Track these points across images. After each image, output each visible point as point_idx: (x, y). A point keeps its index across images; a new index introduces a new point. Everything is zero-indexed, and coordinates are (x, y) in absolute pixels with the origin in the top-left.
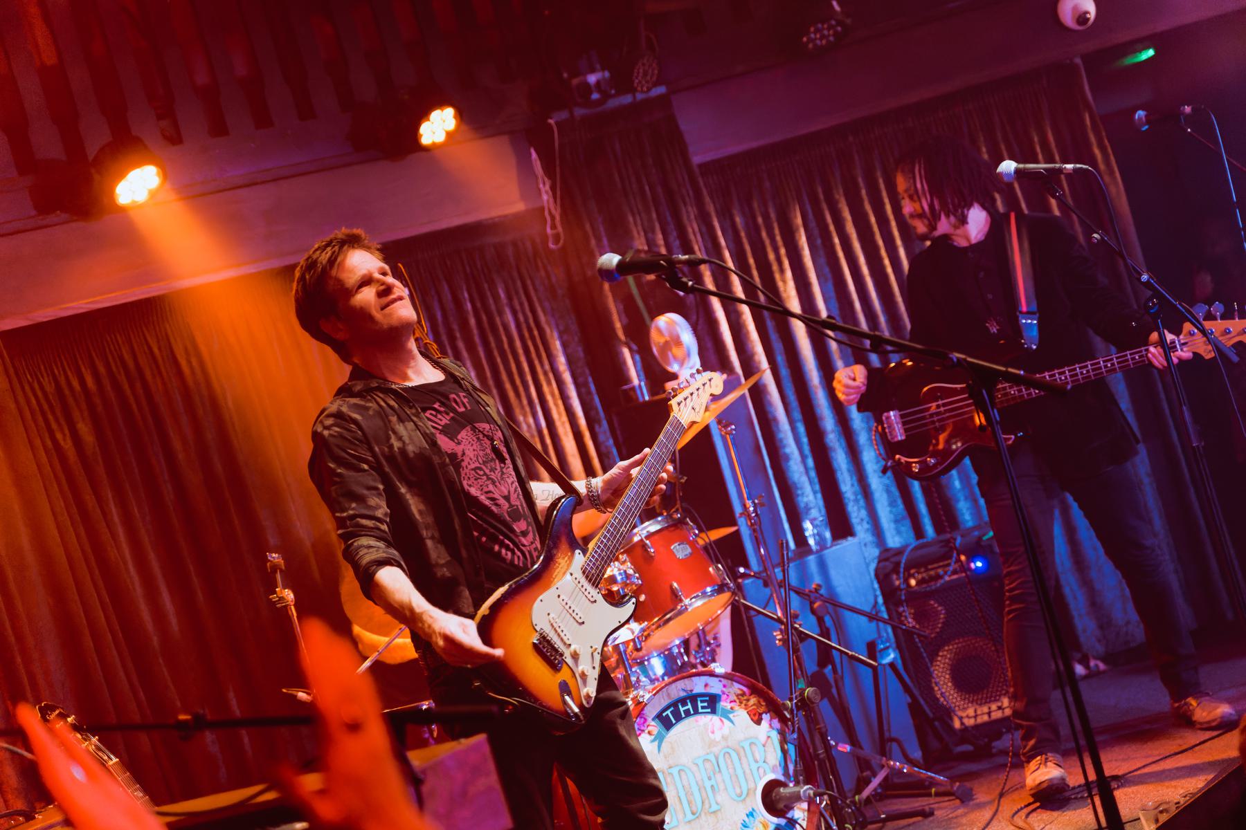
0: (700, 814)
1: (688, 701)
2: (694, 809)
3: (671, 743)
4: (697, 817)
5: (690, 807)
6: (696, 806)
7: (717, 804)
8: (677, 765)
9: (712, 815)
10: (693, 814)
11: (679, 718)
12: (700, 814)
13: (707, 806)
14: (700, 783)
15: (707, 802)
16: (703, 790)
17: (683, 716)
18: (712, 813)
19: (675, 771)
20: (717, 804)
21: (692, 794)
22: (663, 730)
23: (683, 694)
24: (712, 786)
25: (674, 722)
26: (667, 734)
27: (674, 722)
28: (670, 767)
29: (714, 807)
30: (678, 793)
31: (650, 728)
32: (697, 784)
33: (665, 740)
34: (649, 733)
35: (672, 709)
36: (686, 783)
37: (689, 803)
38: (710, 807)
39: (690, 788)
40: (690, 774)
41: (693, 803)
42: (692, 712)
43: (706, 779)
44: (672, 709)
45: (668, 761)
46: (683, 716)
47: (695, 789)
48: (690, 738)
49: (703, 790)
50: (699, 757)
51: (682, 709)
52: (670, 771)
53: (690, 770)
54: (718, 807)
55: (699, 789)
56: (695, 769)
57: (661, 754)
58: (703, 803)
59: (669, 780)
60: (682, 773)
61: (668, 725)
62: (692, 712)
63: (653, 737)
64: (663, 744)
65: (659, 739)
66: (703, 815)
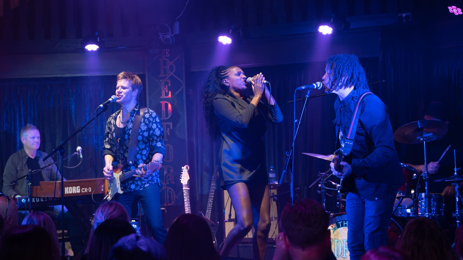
0: (339, 256)
1: (347, 222)
2: (338, 254)
3: (337, 232)
4: (338, 257)
5: (337, 253)
6: (339, 254)
7: (346, 255)
8: (337, 239)
9: (343, 258)
10: (337, 255)
11: (342, 226)
12: (339, 256)
13: (342, 255)
14: (343, 247)
15: (343, 254)
16: (343, 250)
17: (344, 225)
18: (343, 257)
19: (336, 241)
20: (346, 255)
21: (339, 250)
22: (336, 227)
23: (346, 219)
24: (346, 250)
25: (341, 226)
26: (337, 229)
27: (341, 226)
28: (335, 239)
29: (344, 256)
30: (335, 247)
31: (333, 225)
32: (342, 247)
33: (336, 230)
34: (332, 227)
35: (341, 222)
36: (338, 246)
37: (337, 251)
38: (343, 255)
39: (339, 247)
40: (340, 242)
41: (338, 253)
42: (347, 225)
43: (345, 246)
44: (341, 222)
45: (335, 237)
46: (344, 225)
47: (340, 248)
48: (344, 233)
49: (343, 250)
50: (345, 240)
51: (344, 223)
52: (335, 240)
53: (341, 242)
54: (345, 257)
55: (342, 249)
56: (342, 242)
57: (334, 234)
58: (341, 253)
59: (333, 242)
60: (338, 242)
61: (338, 227)
62: (347, 225)
63: (333, 228)
64: (335, 231)
65: (335, 229)
66: (340, 257)
